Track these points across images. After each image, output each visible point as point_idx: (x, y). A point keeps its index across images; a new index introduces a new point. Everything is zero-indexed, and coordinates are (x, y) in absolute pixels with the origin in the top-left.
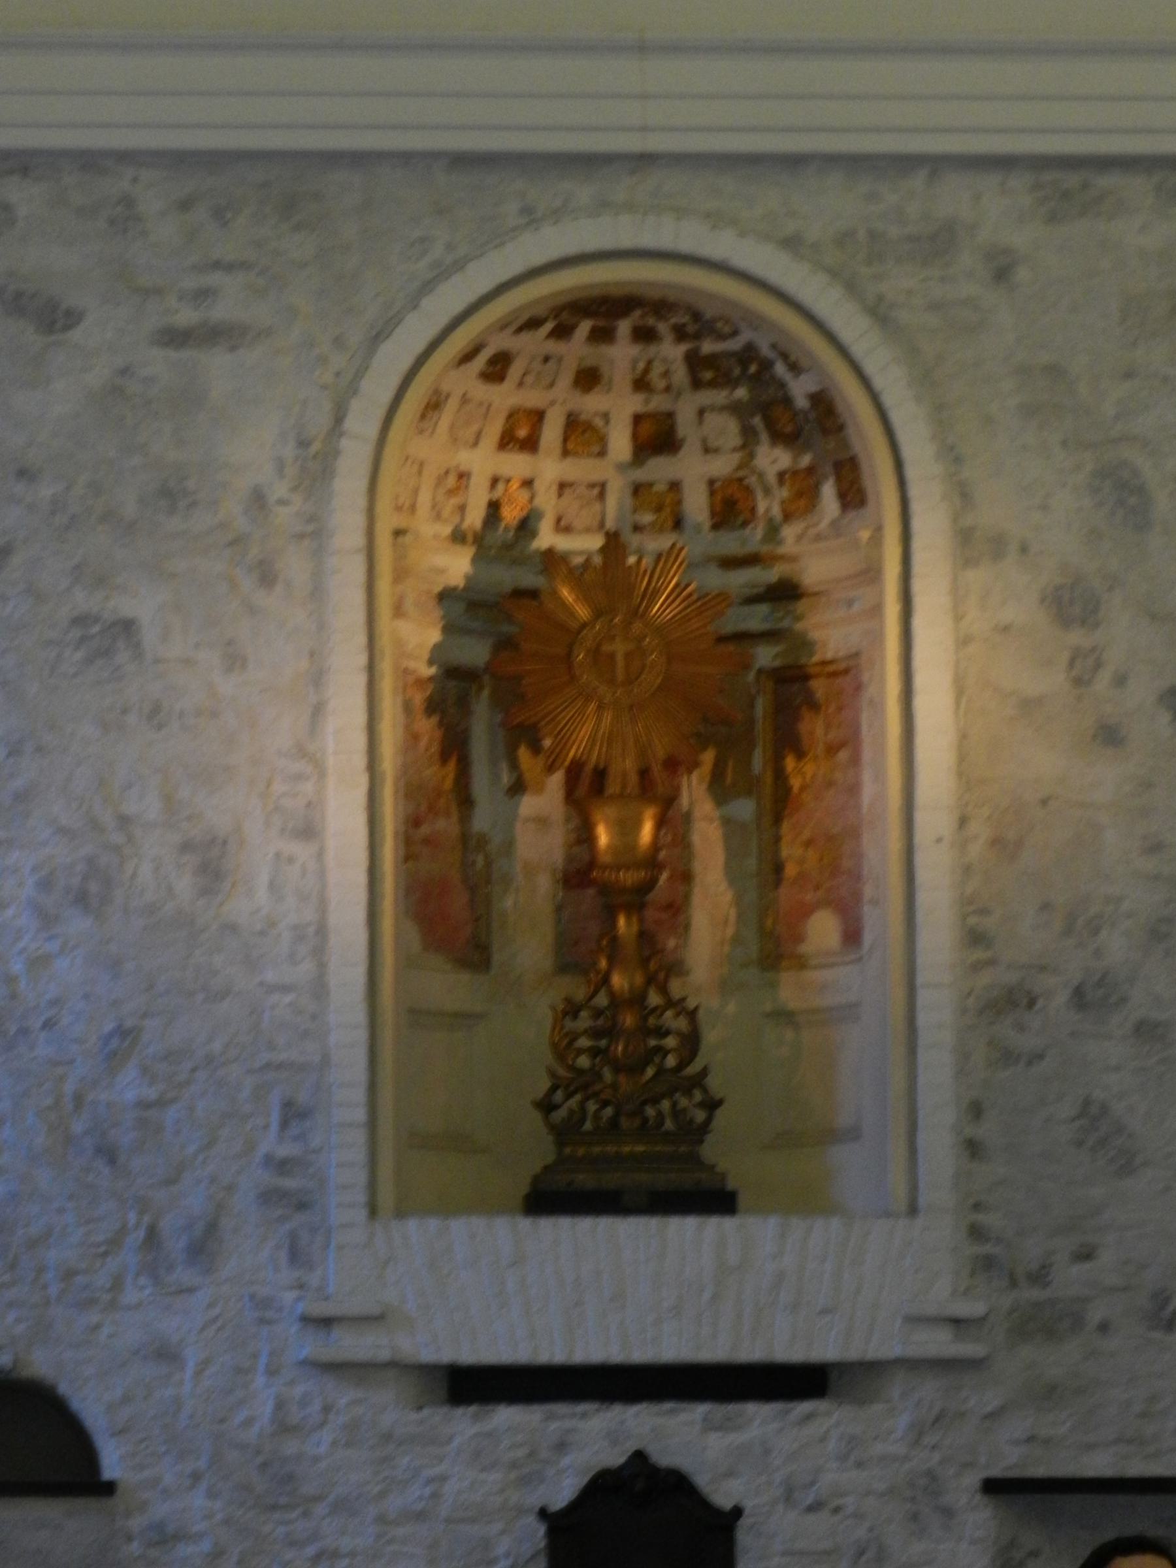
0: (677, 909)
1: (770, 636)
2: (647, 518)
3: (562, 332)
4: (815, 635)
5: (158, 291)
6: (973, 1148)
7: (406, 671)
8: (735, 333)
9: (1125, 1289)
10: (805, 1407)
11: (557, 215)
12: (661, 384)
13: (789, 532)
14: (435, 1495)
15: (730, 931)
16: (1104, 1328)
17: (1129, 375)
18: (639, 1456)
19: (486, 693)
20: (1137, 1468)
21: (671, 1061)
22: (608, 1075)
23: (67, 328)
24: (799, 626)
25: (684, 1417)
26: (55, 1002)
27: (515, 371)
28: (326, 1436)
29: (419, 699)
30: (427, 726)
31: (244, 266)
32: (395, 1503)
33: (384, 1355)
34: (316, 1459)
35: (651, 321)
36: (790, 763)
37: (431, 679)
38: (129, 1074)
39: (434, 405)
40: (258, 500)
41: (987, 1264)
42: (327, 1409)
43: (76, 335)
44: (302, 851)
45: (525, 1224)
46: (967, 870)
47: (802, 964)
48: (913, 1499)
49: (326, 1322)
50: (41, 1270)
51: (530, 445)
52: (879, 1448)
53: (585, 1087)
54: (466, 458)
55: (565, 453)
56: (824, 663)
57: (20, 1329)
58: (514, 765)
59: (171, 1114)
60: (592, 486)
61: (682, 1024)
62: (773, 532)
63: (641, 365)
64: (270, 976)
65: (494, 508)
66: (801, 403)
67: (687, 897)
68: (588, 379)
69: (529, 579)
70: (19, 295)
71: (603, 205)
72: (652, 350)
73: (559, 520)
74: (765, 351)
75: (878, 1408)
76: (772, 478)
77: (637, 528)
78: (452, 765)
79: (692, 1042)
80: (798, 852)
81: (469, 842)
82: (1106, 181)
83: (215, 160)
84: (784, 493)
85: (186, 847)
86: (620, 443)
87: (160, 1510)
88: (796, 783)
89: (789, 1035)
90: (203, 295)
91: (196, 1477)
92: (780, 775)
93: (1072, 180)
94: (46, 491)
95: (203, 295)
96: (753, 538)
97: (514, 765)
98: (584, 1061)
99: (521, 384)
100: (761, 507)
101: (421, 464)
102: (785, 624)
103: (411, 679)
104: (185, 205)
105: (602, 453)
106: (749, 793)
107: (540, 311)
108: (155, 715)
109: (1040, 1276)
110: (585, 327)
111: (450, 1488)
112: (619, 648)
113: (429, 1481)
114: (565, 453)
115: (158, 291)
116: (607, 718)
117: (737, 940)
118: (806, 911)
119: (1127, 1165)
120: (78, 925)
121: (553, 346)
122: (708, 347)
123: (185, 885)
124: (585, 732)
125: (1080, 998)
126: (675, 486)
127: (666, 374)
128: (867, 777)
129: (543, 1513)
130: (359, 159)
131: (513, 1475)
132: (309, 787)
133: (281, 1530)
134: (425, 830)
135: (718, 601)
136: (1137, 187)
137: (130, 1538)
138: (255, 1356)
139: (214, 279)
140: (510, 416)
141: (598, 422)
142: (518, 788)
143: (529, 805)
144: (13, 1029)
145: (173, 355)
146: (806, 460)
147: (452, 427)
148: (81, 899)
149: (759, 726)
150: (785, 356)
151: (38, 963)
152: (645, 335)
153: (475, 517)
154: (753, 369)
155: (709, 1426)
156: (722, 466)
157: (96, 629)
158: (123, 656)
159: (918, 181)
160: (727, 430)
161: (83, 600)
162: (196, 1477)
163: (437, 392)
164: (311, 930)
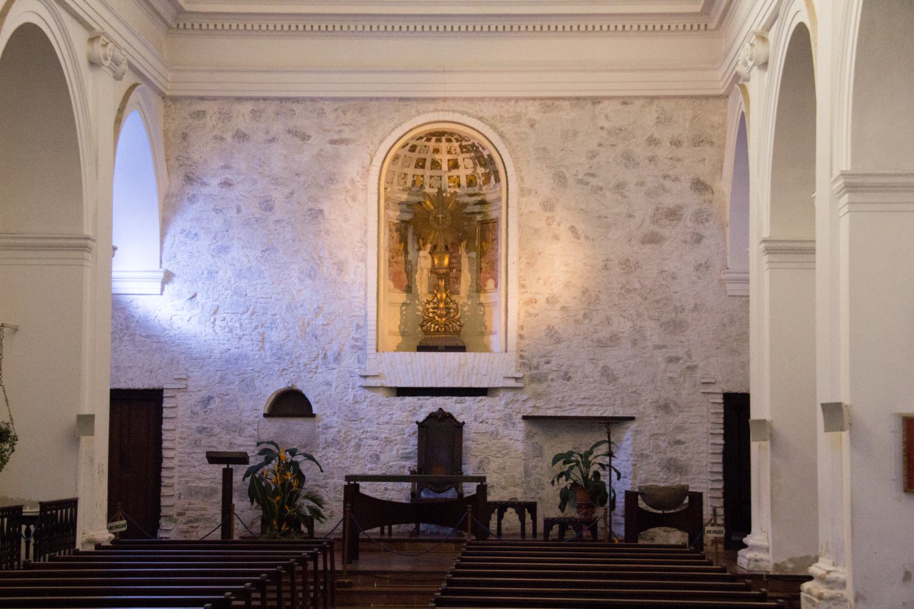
0: (458, 279)
1: (480, 213)
2: (452, 184)
3: (429, 140)
4: (490, 213)
5: (329, 131)
6: (521, 337)
7: (390, 221)
8: (470, 140)
9: (558, 371)
10: (480, 398)
11: (424, 112)
12: (454, 152)
13: (484, 188)
14: (391, 418)
15: (469, 284)
16: (552, 380)
17: (563, 150)
18: (441, 409)
19: (412, 226)
20: (560, 414)
21: (452, 315)
22: (436, 317)
23: (308, 140)
24: (486, 210)
26: (304, 300)
27: (418, 149)
28: (365, 404)
29: (394, 228)
30: (396, 235)
31: (350, 124)
32: (381, 420)
33: (379, 385)
34: (363, 409)
35: (450, 137)
36: (484, 244)
37: (397, 223)
38: (320, 317)
40: (353, 181)
41: (523, 364)
42: (365, 397)
43: (310, 141)
44: (362, 265)
45: (418, 354)
46: (521, 270)
47: (485, 291)
48: (505, 421)
49: (366, 377)
50: (299, 364)
51: (423, 167)
52: (497, 408)
53: (431, 321)
54: (406, 170)
55: (431, 169)
56: (492, 220)
57: (294, 378)
58: (418, 244)
59: (330, 327)
60: (438, 177)
61: (454, 306)
62: (481, 189)
63: (449, 148)
64: (354, 295)
65: (414, 181)
66: (486, 157)
67: (460, 275)
68: (436, 151)
69: (421, 199)
70: (296, 131)
71: (436, 110)
72: (451, 144)
73: (430, 185)
74: (477, 145)
75: (498, 398)
76: (480, 175)
77: (449, 187)
78: (402, 244)
79: (457, 310)
80: (485, 265)
82: (557, 103)
83: (342, 99)
84: (483, 179)
85: (335, 264)
86: (445, 166)
87: (326, 421)
88: (485, 248)
89: (483, 309)
90: (340, 131)
91: (335, 413)
92: (482, 247)
93: (549, 103)
94: (302, 179)
95: (340, 131)
96: (476, 189)
97: (418, 244)
98: (431, 315)
99: (420, 152)
100: (478, 183)
101: (394, 172)
102: (483, 210)
103: (392, 223)
104: (336, 110)
105: (441, 169)
106: (475, 251)
107: (422, 135)
109: (536, 368)
110: (434, 139)
111: (394, 416)
112: (440, 216)
113: (390, 415)
114: (431, 169)
115: (329, 131)
116: (437, 233)
117: (471, 286)
118: (486, 279)
120: (308, 282)
121: (427, 143)
122: (464, 143)
123: (334, 272)
124: (431, 237)
125: (548, 301)
126: (458, 177)
127: (455, 150)
128: (499, 247)
129: (417, 423)
130: (377, 99)
132: (363, 250)
133: (354, 426)
134: (395, 259)
135: (466, 204)
136: (566, 104)
137: (319, 427)
138: (349, 385)
139: (342, 128)
140: (417, 160)
141: (440, 161)
142: (419, 249)
143: (422, 253)
144: (293, 307)
145: (333, 146)
146: (488, 171)
147: (402, 163)
148: (310, 276)
149: (477, 235)
150: (481, 146)
151: (300, 291)
152: (449, 141)
153: (409, 184)
154: (475, 149)
155: (456, 402)
156: (469, 172)
157: (314, 211)
158: (320, 218)
159: (512, 103)
160: (470, 163)
161: (311, 205)
162: (335, 413)
163: (397, 155)
164: (364, 284)
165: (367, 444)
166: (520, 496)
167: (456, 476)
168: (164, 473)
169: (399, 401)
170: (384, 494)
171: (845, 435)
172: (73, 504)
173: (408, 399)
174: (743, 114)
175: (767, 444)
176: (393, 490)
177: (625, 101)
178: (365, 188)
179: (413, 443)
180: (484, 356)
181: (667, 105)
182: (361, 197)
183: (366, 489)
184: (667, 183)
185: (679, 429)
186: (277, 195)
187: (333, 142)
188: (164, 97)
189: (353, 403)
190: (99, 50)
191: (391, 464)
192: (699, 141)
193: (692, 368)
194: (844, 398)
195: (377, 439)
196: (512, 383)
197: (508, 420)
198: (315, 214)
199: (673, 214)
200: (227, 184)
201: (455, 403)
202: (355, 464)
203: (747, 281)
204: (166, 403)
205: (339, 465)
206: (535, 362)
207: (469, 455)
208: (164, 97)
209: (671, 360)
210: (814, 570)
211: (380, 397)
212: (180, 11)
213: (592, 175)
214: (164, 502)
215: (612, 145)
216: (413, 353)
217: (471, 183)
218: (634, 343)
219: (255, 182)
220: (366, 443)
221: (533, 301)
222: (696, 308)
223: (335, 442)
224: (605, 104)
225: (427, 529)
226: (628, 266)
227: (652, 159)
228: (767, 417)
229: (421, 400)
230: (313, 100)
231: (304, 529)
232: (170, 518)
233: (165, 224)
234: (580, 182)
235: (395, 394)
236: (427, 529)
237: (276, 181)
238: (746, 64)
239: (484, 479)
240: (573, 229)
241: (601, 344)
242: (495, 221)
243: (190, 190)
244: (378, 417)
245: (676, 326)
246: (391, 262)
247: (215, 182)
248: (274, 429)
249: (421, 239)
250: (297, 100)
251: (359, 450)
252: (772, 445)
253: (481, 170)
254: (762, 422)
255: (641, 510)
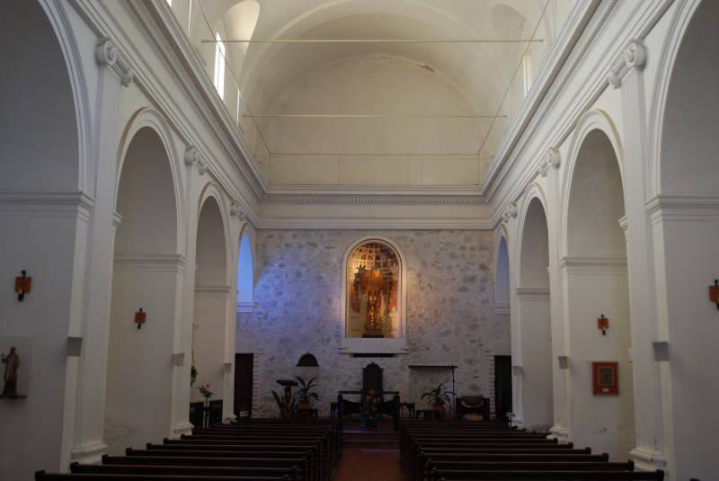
0: (379, 306)
6: (407, 331)
39: (354, 255)
49: (340, 349)
68: (370, 252)
79: (380, 320)
81: (358, 299)
86: (374, 258)
108: (324, 286)
119: (424, 333)
166: (409, 401)
167: (381, 392)
168: (254, 390)
169: (355, 359)
171: (567, 371)
172: (220, 402)
173: (360, 359)
174: (503, 239)
175: (521, 376)
177: (451, 231)
178: (341, 268)
179: (361, 379)
180: (392, 340)
181: (468, 233)
182: (339, 271)
183: (345, 397)
184: (470, 266)
185: (476, 371)
186: (303, 270)
187: (327, 248)
188: (256, 229)
190: (235, 208)
192: (482, 248)
193: (481, 345)
194: (567, 353)
196: (404, 351)
197: (402, 368)
198: (320, 278)
199: (473, 279)
200: (281, 266)
203: (509, 307)
204: (255, 360)
206: (414, 342)
208: (256, 229)
209: (473, 341)
210: (551, 430)
211: (347, 357)
212: (264, 193)
213: (437, 262)
214: (253, 403)
215: (446, 250)
216: (359, 339)
217: (385, 265)
218: (456, 334)
219: (293, 265)
221: (412, 316)
222: (483, 319)
224: (443, 234)
226: (454, 301)
227: (463, 256)
228: (520, 365)
230: (319, 230)
231: (314, 415)
232: (256, 410)
233: (255, 282)
234: (433, 265)
237: (303, 265)
238: (506, 214)
239: (398, 393)
240: (430, 285)
241: (442, 334)
242: (396, 282)
243: (267, 268)
245: (474, 327)
246: (351, 300)
247: (277, 265)
248: (301, 371)
249: (364, 289)
250: (312, 230)
252: (523, 378)
253: (389, 260)
254: (516, 367)
255: (463, 407)
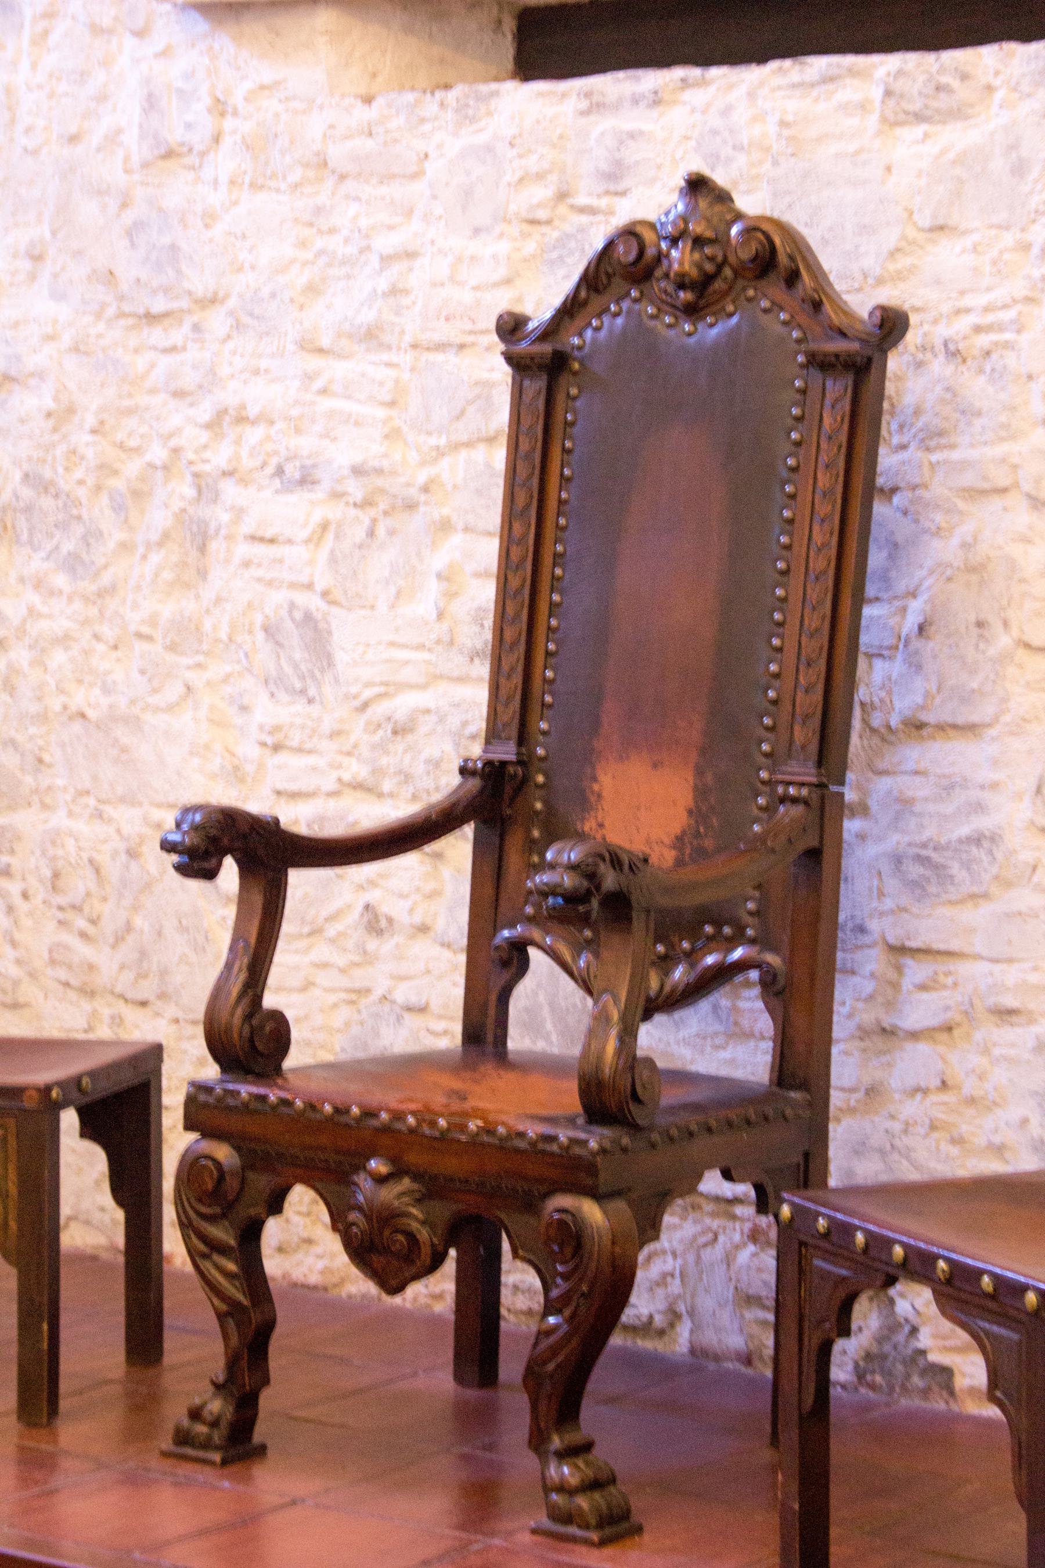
14: (395, 291)
25: (849, 92)
42: (220, 108)
113: (387, 260)
131: (530, 247)
133: (165, 362)
165: (247, 527)
170: (367, 959)
176: (423, 929)
189: (145, 165)
191: (403, 704)
195: (306, 481)
201: (890, 123)
202: (173, 692)
205: (79, 699)
207: (1004, 641)
220: (239, 512)
223: (47, 502)
225: (674, 1316)
229: (616, 107)
235: (507, 48)
236: (674, 1316)
244: (312, 289)
251: (203, 574)
